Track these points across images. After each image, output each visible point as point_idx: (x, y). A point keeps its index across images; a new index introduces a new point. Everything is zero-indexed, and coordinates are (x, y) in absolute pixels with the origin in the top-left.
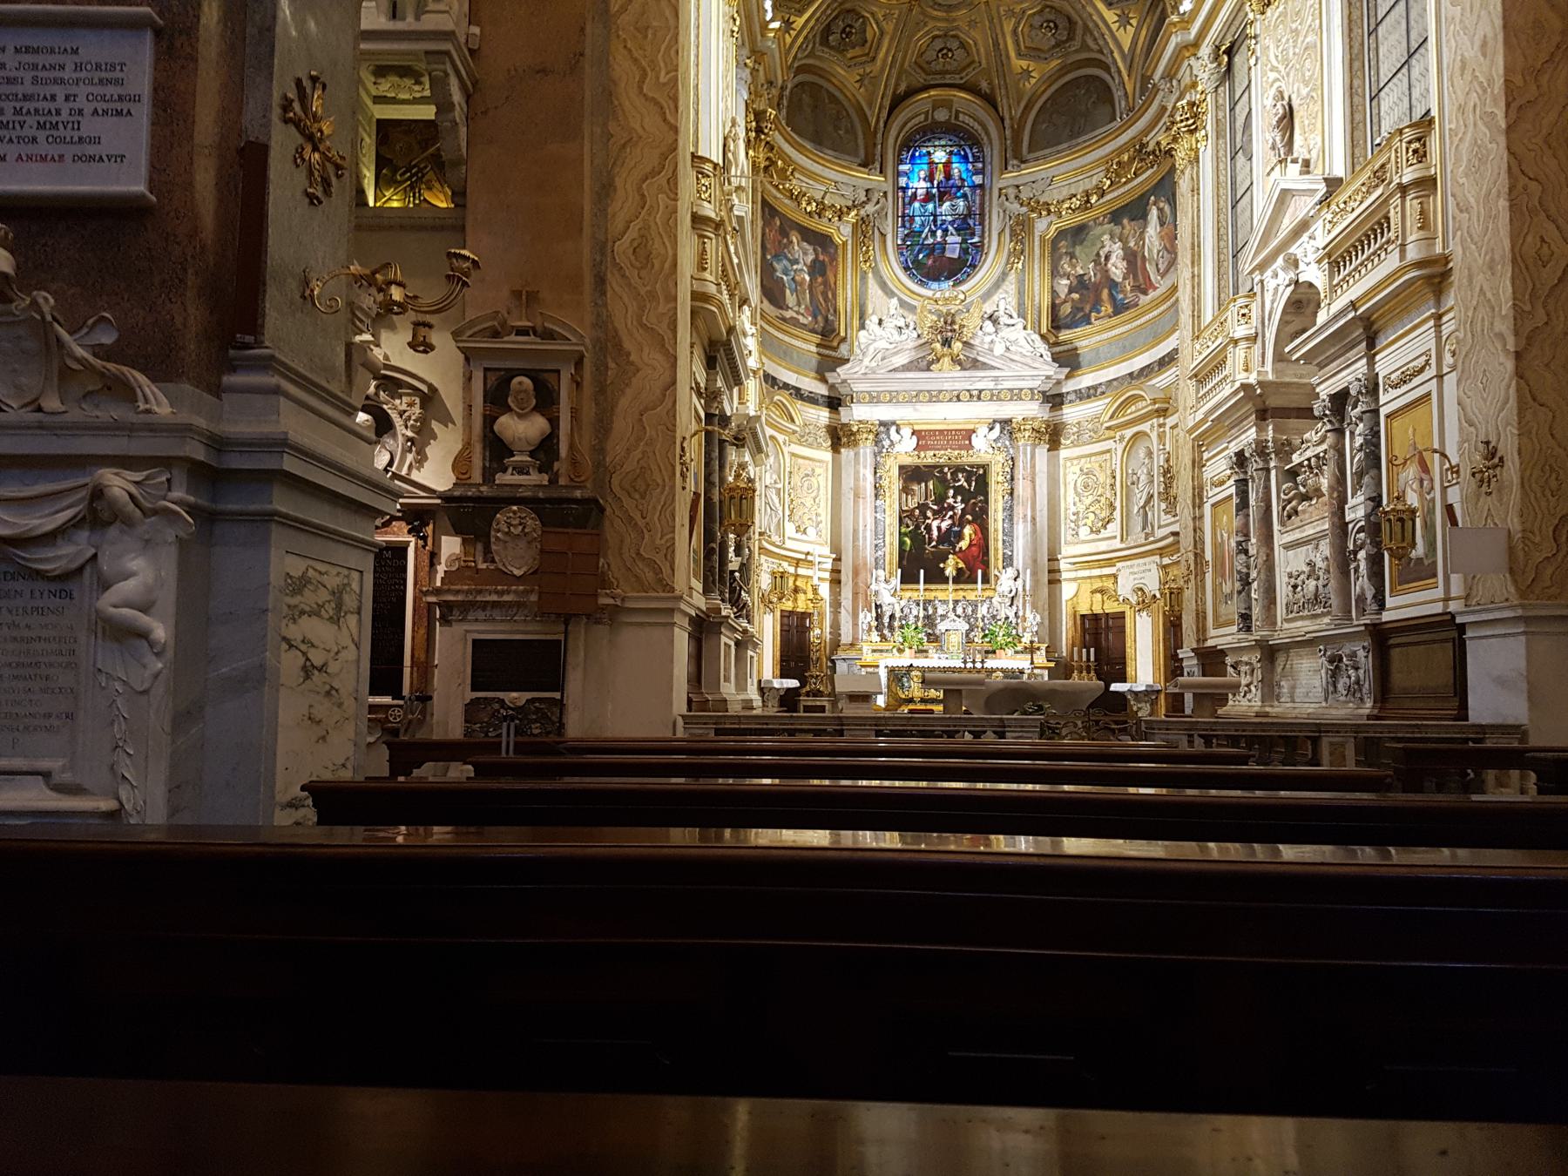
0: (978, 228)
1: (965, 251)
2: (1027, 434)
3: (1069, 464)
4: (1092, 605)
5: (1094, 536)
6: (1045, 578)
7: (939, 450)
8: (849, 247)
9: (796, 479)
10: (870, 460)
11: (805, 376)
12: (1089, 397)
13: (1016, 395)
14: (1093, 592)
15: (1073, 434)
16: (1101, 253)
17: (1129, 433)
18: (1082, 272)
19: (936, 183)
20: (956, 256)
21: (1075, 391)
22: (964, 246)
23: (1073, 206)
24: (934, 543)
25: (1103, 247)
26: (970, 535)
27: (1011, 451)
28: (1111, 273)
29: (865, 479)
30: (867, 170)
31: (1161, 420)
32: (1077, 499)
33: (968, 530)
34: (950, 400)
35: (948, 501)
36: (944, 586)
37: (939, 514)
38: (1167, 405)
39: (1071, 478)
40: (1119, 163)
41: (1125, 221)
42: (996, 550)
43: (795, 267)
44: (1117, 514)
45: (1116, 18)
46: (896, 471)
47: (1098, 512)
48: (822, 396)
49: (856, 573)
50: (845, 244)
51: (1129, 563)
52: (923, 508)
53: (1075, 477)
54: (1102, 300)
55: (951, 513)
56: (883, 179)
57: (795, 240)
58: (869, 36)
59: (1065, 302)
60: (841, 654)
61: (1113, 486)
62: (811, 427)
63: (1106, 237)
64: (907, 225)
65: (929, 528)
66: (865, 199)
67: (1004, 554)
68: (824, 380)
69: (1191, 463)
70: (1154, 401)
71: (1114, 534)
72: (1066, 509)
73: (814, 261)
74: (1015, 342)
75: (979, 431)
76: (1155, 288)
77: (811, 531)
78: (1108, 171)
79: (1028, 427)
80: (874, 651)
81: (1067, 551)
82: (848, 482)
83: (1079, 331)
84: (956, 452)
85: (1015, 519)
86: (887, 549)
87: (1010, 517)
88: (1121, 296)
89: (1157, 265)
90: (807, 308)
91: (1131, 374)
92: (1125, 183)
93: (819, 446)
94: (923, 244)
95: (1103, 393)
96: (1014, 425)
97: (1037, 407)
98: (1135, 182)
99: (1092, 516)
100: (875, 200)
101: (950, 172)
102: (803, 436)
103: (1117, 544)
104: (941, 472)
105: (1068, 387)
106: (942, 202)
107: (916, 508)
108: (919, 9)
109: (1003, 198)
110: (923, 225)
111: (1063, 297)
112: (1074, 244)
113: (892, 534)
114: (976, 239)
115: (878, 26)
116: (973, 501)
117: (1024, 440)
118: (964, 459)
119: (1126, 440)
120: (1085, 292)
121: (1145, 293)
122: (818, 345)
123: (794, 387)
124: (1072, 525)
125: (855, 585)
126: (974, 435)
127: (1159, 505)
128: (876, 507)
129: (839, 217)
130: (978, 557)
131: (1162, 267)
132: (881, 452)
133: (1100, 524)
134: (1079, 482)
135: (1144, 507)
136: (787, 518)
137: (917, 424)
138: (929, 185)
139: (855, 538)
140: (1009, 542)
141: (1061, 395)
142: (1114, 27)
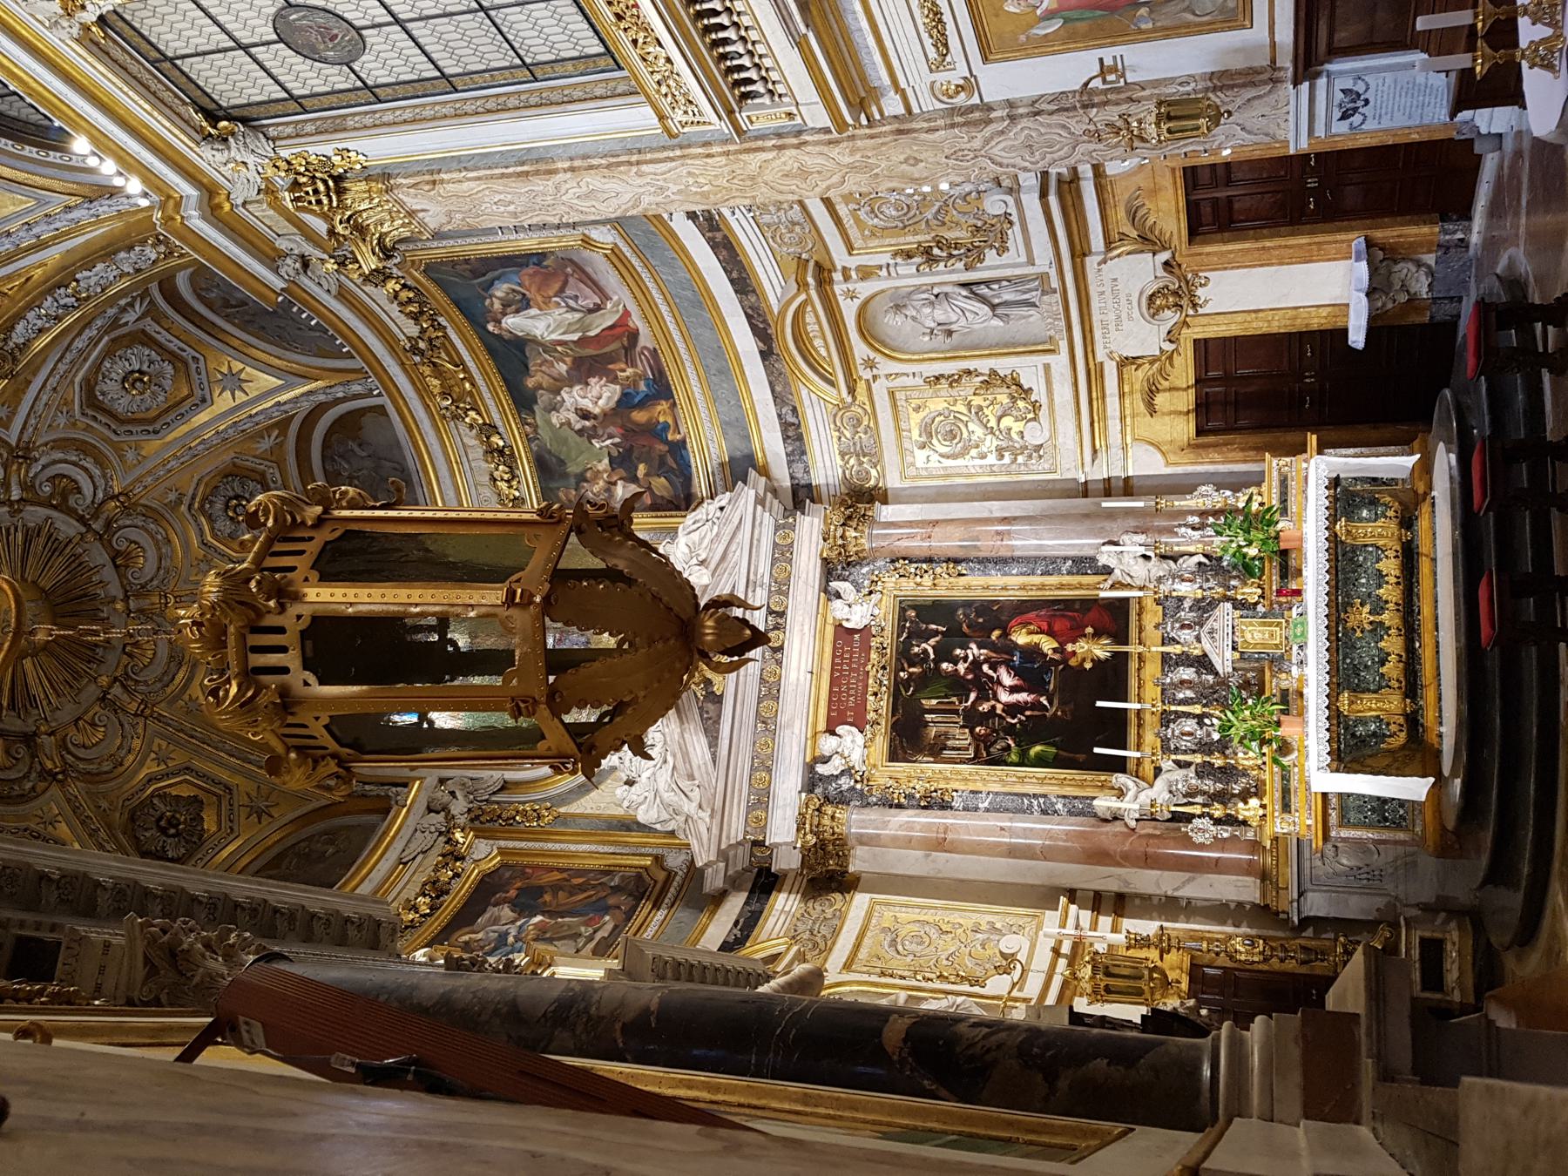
2: (851, 533)
5: (1044, 413)
7: (867, 686)
8: (511, 844)
9: (898, 964)
10: (873, 814)
11: (703, 931)
12: (800, 438)
13: (783, 553)
14: (1152, 410)
15: (861, 463)
16: (578, 427)
17: (860, 350)
18: (606, 461)
21: (790, 463)
23: (506, 477)
25: (569, 423)
26: (1030, 633)
27: (880, 563)
28: (607, 408)
30: (395, 808)
31: (837, 276)
32: (974, 452)
34: (779, 663)
35: (962, 671)
36: (1133, 665)
37: (986, 688)
38: (811, 264)
40: (445, 394)
41: (530, 383)
42: (1061, 587)
43: (511, 939)
44: (1004, 365)
45: (227, 394)
47: (998, 409)
48: (746, 903)
49: (1100, 856)
50: (502, 851)
51: (1098, 334)
52: (972, 719)
53: (934, 457)
54: (650, 419)
55: (985, 668)
57: (466, 938)
58: (186, 792)
60: (1286, 902)
61: (954, 380)
62: (801, 928)
63: (555, 419)
65: (1012, 709)
66: (443, 813)
67: (1069, 573)
68: (718, 899)
69: (904, 139)
70: (802, 285)
71: (1041, 368)
72: (992, 473)
73: (515, 905)
75: (839, 615)
76: (627, 313)
77: (1009, 944)
78: (455, 417)
79: (840, 532)
80: (1286, 807)
82: (912, 863)
84: (874, 656)
85: (1004, 553)
87: (1002, 562)
88: (642, 387)
89: (590, 311)
90: (587, 924)
91: (761, 352)
92: (473, 384)
93: (842, 916)
96: (834, 555)
97: (808, 519)
98: (471, 364)
99: (1007, 422)
100: (447, 798)
102: (815, 945)
103: (1060, 362)
104: (906, 684)
105: (782, 475)
108: (163, 704)
112: (565, 476)
113: (1022, 780)
115: (174, 775)
117: (860, 539)
119: (872, 355)
121: (634, 335)
122: (657, 906)
125: (1126, 859)
126: (846, 624)
129: (457, 859)
131: (592, 299)
132: (861, 794)
133: (1021, 404)
135: (993, 307)
136: (976, 989)
137: (815, 724)
140: (1050, 564)
141: (795, 489)
142: (241, 397)
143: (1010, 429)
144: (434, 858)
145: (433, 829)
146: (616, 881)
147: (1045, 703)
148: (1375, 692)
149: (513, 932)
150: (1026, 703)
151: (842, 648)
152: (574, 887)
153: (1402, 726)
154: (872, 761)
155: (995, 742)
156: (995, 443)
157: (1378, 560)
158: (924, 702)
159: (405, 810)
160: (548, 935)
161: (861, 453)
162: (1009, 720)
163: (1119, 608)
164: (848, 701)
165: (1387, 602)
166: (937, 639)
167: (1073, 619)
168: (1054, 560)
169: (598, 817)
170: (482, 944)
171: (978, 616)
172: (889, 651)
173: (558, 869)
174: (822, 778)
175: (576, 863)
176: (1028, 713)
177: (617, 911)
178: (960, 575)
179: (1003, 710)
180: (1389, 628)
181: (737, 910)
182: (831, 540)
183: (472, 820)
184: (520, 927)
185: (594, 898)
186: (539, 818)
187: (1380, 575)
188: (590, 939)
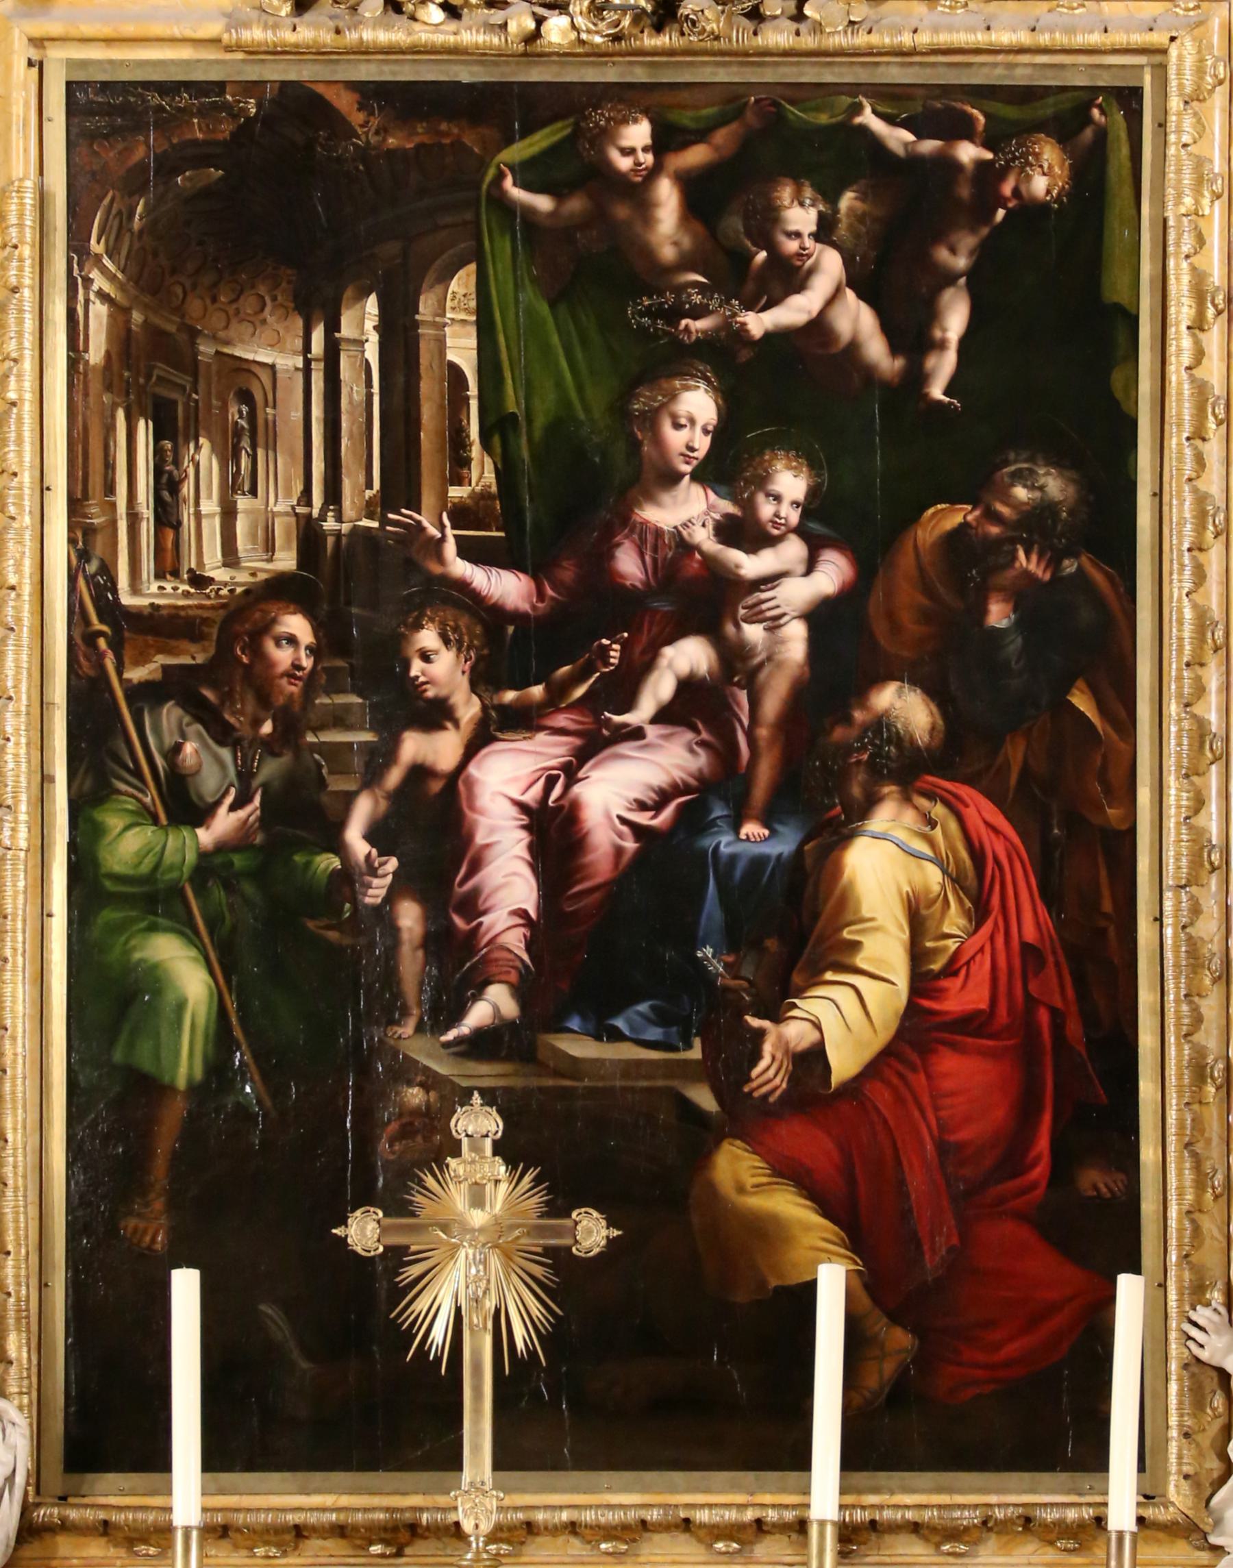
147: (478, 1015)
150: (472, 906)
155: (222, 733)
158: (462, 284)
162: (363, 811)
166: (876, 349)
176: (409, 916)
179: (420, 772)
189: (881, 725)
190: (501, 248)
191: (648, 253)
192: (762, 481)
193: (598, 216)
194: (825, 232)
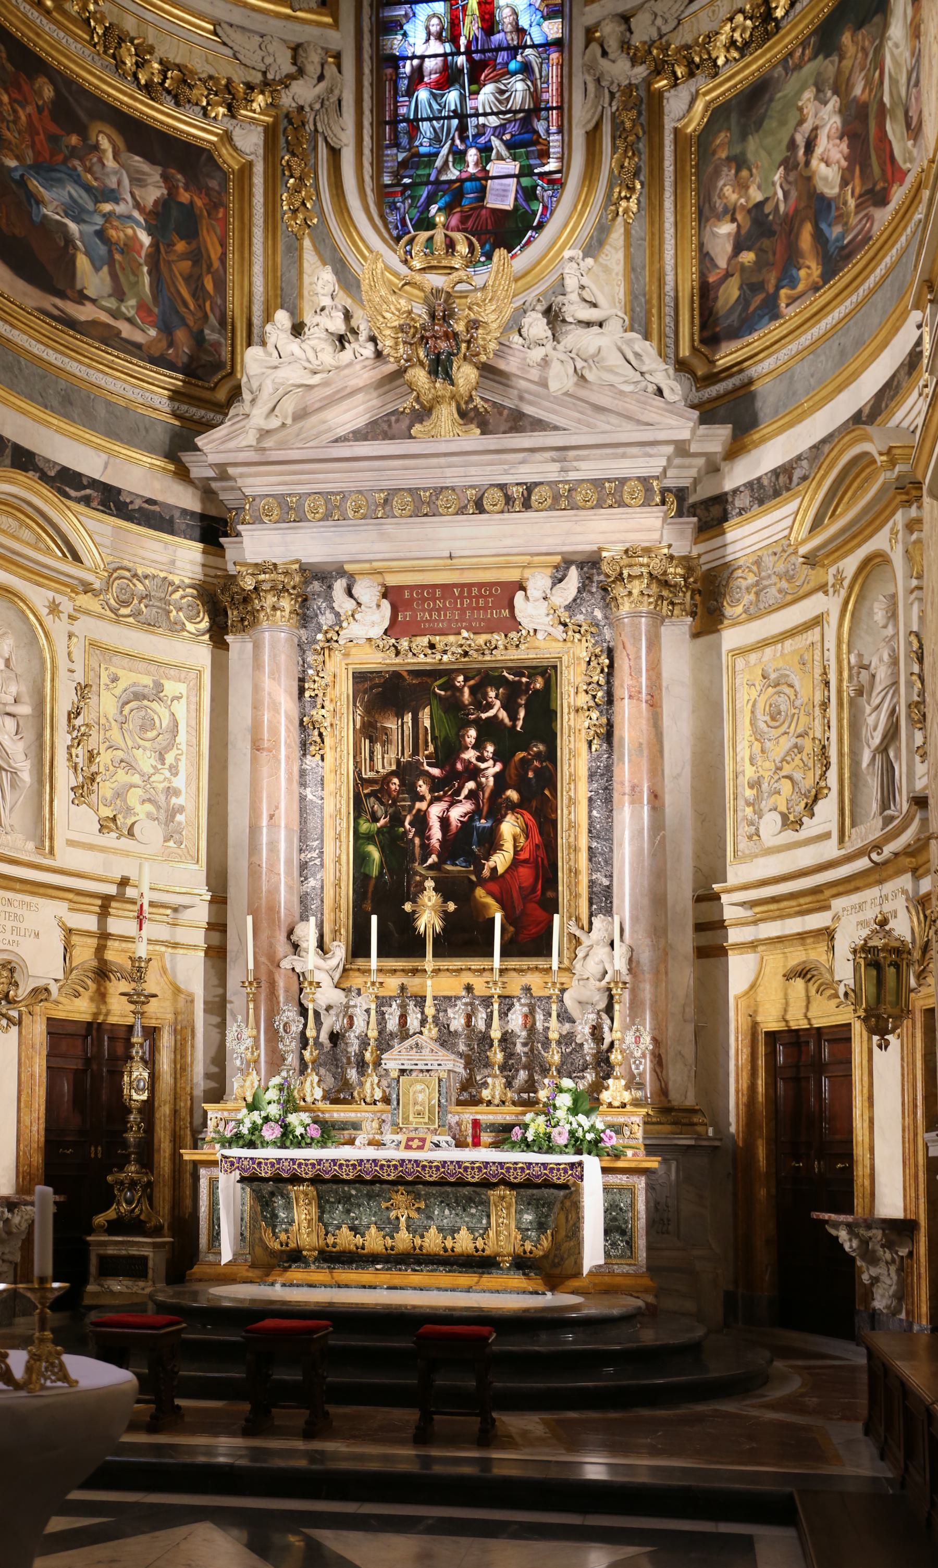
0: (555, 140)
1: (529, 194)
2: (636, 587)
3: (740, 663)
4: (786, 1011)
5: (790, 836)
6: (685, 941)
14: (788, 977)
19: (463, 41)
20: (508, 204)
21: (750, 485)
22: (525, 181)
24: (433, 859)
29: (275, 707)
33: (509, 827)
34: (461, 511)
39: (745, 696)
44: (832, 775)
46: (345, 687)
47: (797, 776)
51: (855, 898)
56: (328, 20)
59: (728, 275)
64: (404, 141)
66: (293, 69)
68: (182, 474)
74: (595, 358)
81: (736, 873)
83: (756, 340)
84: (481, 639)
85: (616, 795)
86: (328, 875)
94: (438, 182)
95: (804, 478)
96: (605, 568)
97: (658, 523)
99: (786, 786)
101: (492, 15)
103: (831, 850)
106: (476, 81)
107: (393, 773)
109: (595, 48)
110: (437, 139)
111: (722, 263)
114: (552, 165)
116: (521, 755)
118: (499, 655)
119: (846, 583)
120: (766, 243)
123: (95, 484)
124: (749, 811)
126: (519, 595)
127: (911, 738)
128: (303, 773)
129: (230, 107)
130: (534, 890)
134: (760, 705)
138: (448, 48)
139: (254, 848)
143: (779, 793)
144: (225, 70)
145: (269, 60)
146: (211, 335)
148: (320, 1219)
149: (120, 209)
151: (491, 595)
152: (200, 278)
153: (287, 1245)
154: (353, 651)
156: (767, 775)
157: (471, 1230)
159: (288, 11)
160: (117, 257)
161: (759, 589)
163: (541, 947)
164: (424, 610)
165: (422, 1237)
166: (507, 720)
167: (534, 890)
168: (609, 862)
169: (300, 296)
170: (97, 168)
171: (537, 771)
172: (488, 658)
173: (224, 254)
174: (330, 587)
175: (233, 275)
177: (164, 344)
178: (590, 743)
180: (392, 1238)
181: (171, 500)
182: (626, 561)
183: (287, 116)
184: (130, 217)
185: (183, 310)
186: (295, 211)
187: (454, 1231)
188: (116, 314)
189: (508, 798)
190: (435, 702)
191: (463, 702)
192: (485, 748)
193: (453, 695)
194: (497, 697)
